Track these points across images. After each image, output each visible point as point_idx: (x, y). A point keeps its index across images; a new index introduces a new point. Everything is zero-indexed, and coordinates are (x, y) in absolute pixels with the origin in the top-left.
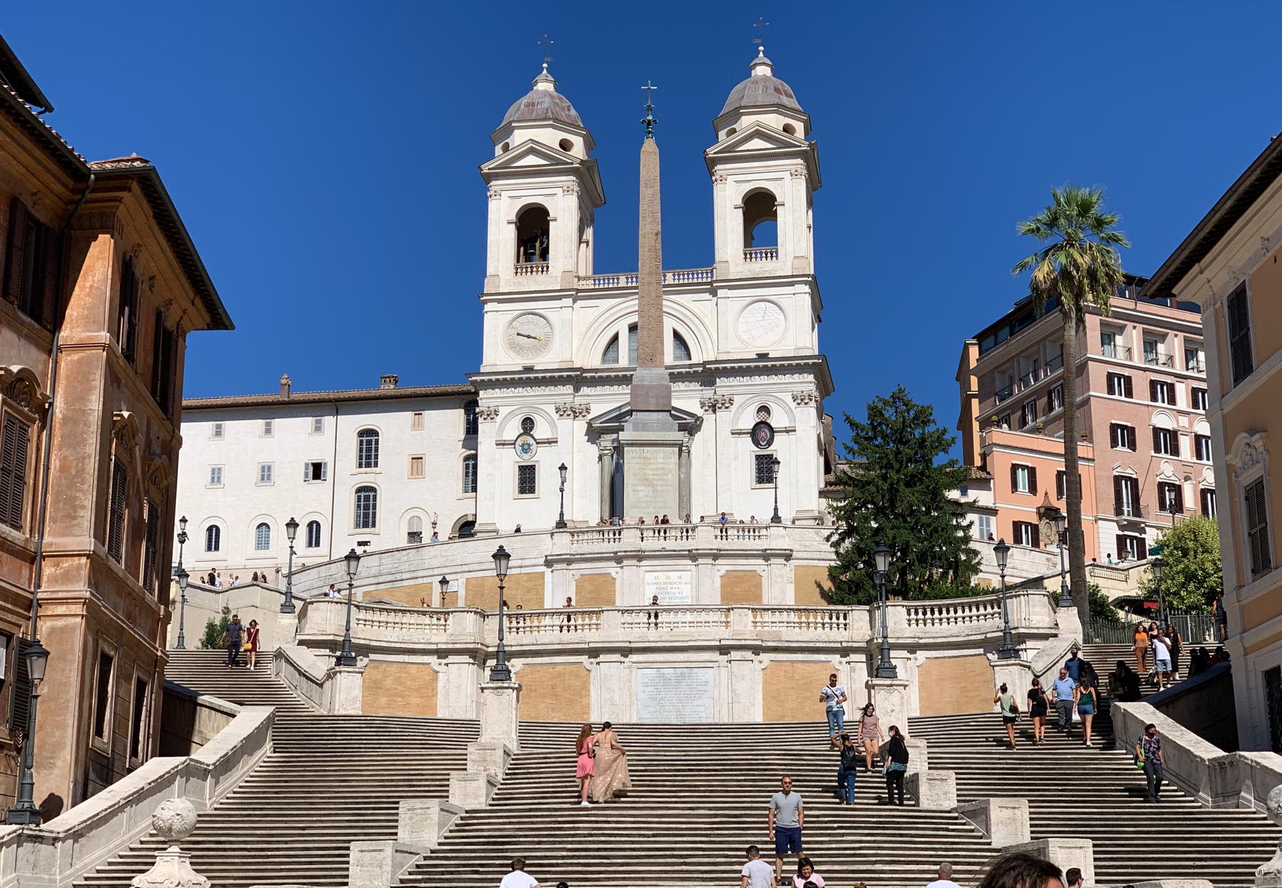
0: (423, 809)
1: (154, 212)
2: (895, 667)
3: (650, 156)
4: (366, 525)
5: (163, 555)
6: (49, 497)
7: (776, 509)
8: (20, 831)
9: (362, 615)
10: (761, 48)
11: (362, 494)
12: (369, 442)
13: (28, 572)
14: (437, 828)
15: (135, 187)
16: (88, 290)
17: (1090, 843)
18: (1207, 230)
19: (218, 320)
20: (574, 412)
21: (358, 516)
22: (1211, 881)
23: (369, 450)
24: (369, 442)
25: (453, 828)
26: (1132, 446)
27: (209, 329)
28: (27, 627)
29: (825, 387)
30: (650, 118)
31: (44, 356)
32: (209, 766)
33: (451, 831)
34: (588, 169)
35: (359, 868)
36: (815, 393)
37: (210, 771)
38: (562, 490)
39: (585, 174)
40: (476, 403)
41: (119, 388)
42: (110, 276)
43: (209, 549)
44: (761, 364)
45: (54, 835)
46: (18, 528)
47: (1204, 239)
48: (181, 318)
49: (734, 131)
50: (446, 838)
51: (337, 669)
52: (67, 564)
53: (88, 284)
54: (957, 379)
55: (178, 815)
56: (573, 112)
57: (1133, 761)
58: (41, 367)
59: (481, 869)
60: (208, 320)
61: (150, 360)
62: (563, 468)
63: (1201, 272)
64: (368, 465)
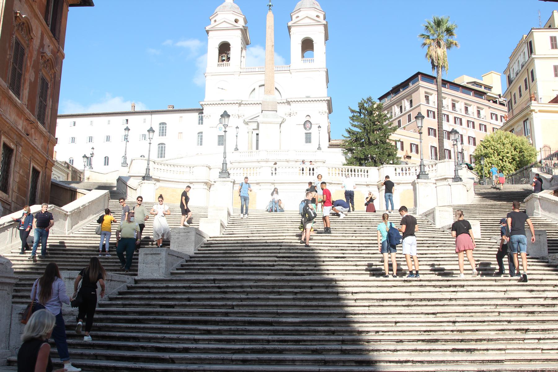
0: (185, 232)
2: (428, 174)
3: (270, 18)
4: (161, 157)
5: (52, 109)
9: (156, 166)
11: (160, 146)
12: (163, 127)
14: (194, 244)
20: (239, 116)
21: (159, 154)
23: (163, 130)
24: (163, 127)
25: (203, 245)
32: (67, 212)
33: (201, 247)
35: (145, 265)
37: (68, 216)
38: (237, 136)
40: (202, 113)
50: (199, 250)
51: (143, 182)
56: (239, 10)
57: (455, 243)
62: (237, 128)
64: (163, 135)
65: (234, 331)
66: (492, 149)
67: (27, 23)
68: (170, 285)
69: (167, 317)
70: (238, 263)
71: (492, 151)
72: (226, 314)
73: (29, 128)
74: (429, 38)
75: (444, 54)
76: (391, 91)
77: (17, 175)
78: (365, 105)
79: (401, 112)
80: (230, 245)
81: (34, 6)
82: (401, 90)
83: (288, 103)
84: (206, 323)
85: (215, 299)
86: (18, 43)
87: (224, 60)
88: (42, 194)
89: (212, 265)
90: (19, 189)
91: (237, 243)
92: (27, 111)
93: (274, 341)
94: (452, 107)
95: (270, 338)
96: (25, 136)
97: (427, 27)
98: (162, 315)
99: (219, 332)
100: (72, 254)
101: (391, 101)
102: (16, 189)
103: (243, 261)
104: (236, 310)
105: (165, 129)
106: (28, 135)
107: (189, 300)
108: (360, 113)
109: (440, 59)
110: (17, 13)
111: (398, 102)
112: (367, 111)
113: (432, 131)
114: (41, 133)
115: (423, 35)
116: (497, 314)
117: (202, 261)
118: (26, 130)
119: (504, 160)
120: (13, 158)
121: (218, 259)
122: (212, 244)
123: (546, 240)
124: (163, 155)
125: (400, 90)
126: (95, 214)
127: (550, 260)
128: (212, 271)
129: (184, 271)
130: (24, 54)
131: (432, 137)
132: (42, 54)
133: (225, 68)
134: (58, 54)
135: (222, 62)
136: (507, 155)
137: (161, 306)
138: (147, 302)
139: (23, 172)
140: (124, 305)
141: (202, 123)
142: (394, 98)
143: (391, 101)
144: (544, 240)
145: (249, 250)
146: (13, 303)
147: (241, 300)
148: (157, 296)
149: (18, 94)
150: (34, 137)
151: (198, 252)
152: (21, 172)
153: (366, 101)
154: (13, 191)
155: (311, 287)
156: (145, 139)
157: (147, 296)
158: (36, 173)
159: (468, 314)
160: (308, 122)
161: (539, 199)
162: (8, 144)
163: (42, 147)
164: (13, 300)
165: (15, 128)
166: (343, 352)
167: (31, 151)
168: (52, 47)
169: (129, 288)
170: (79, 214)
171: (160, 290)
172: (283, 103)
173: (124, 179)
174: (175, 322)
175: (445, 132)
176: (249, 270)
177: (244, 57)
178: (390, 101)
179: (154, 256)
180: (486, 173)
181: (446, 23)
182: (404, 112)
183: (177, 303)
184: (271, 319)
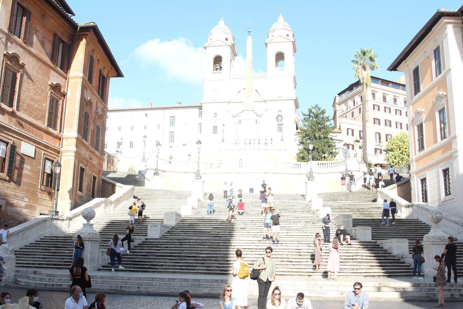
1: (98, 40)
4: (171, 142)
6: (65, 121)
7: (282, 137)
8: (52, 217)
10: (281, 14)
11: (171, 133)
12: (173, 119)
13: (59, 143)
15: (91, 31)
16: (77, 61)
17: (370, 228)
18: (408, 49)
19: (119, 74)
22: (408, 239)
23: (172, 121)
24: (173, 119)
25: (180, 221)
26: (379, 124)
27: (117, 77)
28: (58, 159)
29: (297, 106)
30: (250, 31)
31: (64, 80)
33: (179, 222)
34: (233, 46)
36: (294, 108)
39: (233, 47)
40: (201, 109)
41: (87, 90)
42: (84, 57)
43: (130, 147)
44: (279, 99)
45: (63, 219)
46: (56, 130)
47: (407, 52)
48: (108, 73)
49: (273, 36)
50: (178, 223)
52: (70, 141)
53: (77, 60)
54: (333, 106)
55: (89, 212)
56: (229, 30)
58: (63, 83)
59: (187, 233)
60: (116, 74)
61: (98, 83)
63: (406, 62)
64: (172, 125)
65: (181, 259)
66: (395, 146)
67: (90, 101)
68: (160, 241)
69: (157, 254)
70: (194, 231)
71: (395, 147)
72: (180, 253)
73: (91, 155)
74: (358, 64)
75: (368, 75)
76: (347, 89)
77: (86, 181)
78: (314, 110)
79: (354, 106)
80: (193, 221)
81: (93, 90)
82: (354, 88)
83: (265, 101)
84: (171, 256)
85: (177, 247)
86: (86, 113)
87: (218, 69)
88: (97, 189)
89: (182, 231)
90: (87, 188)
91: (197, 220)
92: (90, 147)
93: (194, 263)
94: (394, 101)
95: (193, 262)
96: (89, 160)
97: (356, 56)
98: (156, 253)
99: (175, 260)
100: (116, 225)
101: (347, 97)
102: (86, 189)
103: (197, 230)
104: (184, 252)
105: (174, 120)
106: (91, 159)
107: (167, 247)
108: (309, 115)
109: (364, 79)
110: (85, 98)
111: (353, 97)
112: (314, 115)
113: (377, 120)
114: (97, 156)
115: (353, 61)
116: (286, 255)
117: (178, 229)
118: (90, 157)
119: (403, 154)
120: (85, 173)
121: (185, 228)
122: (185, 220)
123: (352, 220)
124: (173, 140)
125: (353, 89)
126: (127, 200)
127: (348, 231)
128: (181, 234)
129: (168, 234)
130: (89, 117)
131: (377, 125)
132: (97, 113)
133: (218, 75)
134: (105, 109)
135: (217, 70)
136: (406, 150)
137: (155, 250)
138: (150, 248)
139: (89, 179)
140: (141, 249)
141: (201, 117)
142: (348, 94)
143: (347, 97)
144: (351, 221)
145: (201, 223)
146: (100, 248)
147: (187, 248)
148: (154, 246)
149: (86, 139)
150: (93, 159)
151: (177, 224)
152: (88, 180)
153: (314, 107)
154: (85, 190)
155: (218, 243)
156: (159, 129)
157: (150, 246)
158: (95, 178)
159: (274, 255)
160: (279, 116)
161: (380, 192)
162: (82, 167)
163: (97, 163)
164: (100, 247)
165: (85, 158)
166: (218, 267)
167: (92, 167)
168: (102, 106)
169: (143, 242)
170: (118, 201)
171: (156, 243)
172: (261, 101)
173: (143, 173)
174: (160, 256)
175: (388, 122)
176: (198, 234)
177: (233, 66)
178: (346, 97)
179: (155, 227)
180: (390, 163)
181: (370, 53)
182: (356, 106)
183: (161, 249)
184: (195, 255)
